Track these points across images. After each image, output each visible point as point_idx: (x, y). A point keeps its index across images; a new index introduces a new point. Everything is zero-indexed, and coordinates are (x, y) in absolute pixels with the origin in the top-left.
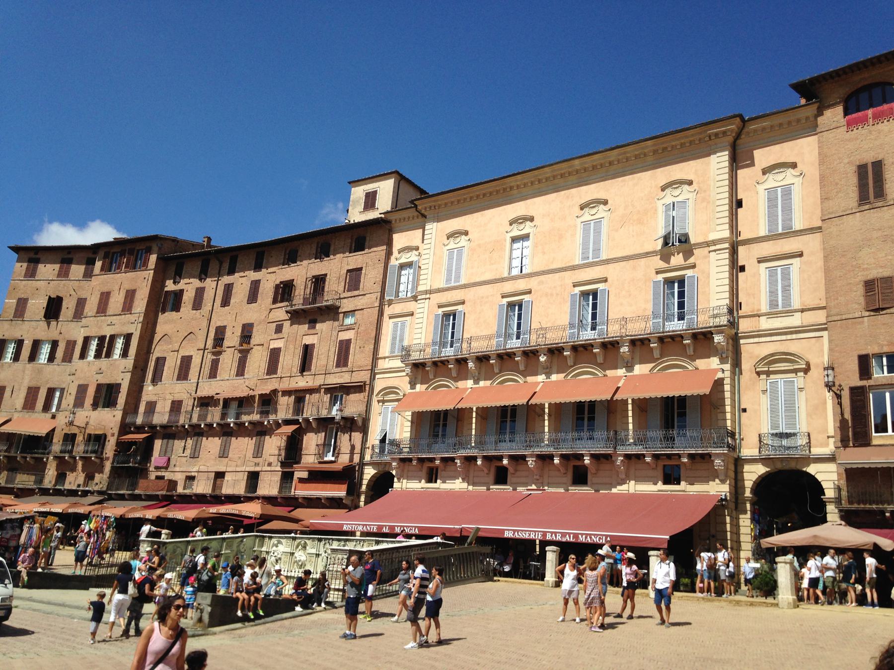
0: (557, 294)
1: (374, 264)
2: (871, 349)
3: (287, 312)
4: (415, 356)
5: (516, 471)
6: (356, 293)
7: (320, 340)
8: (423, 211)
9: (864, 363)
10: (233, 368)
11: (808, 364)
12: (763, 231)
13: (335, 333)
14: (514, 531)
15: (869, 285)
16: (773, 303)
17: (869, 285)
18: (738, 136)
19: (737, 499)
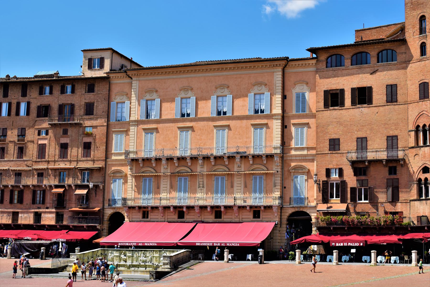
0: (206, 130)
1: (102, 101)
2: (330, 167)
3: (49, 124)
4: (132, 156)
5: (188, 213)
6: (92, 116)
7: (71, 141)
8: (130, 76)
9: (328, 172)
10: (15, 154)
11: (309, 170)
12: (294, 112)
13: (80, 138)
14: (200, 243)
15: (330, 140)
16: (297, 144)
17: (330, 140)
18: (286, 66)
19: (281, 223)
